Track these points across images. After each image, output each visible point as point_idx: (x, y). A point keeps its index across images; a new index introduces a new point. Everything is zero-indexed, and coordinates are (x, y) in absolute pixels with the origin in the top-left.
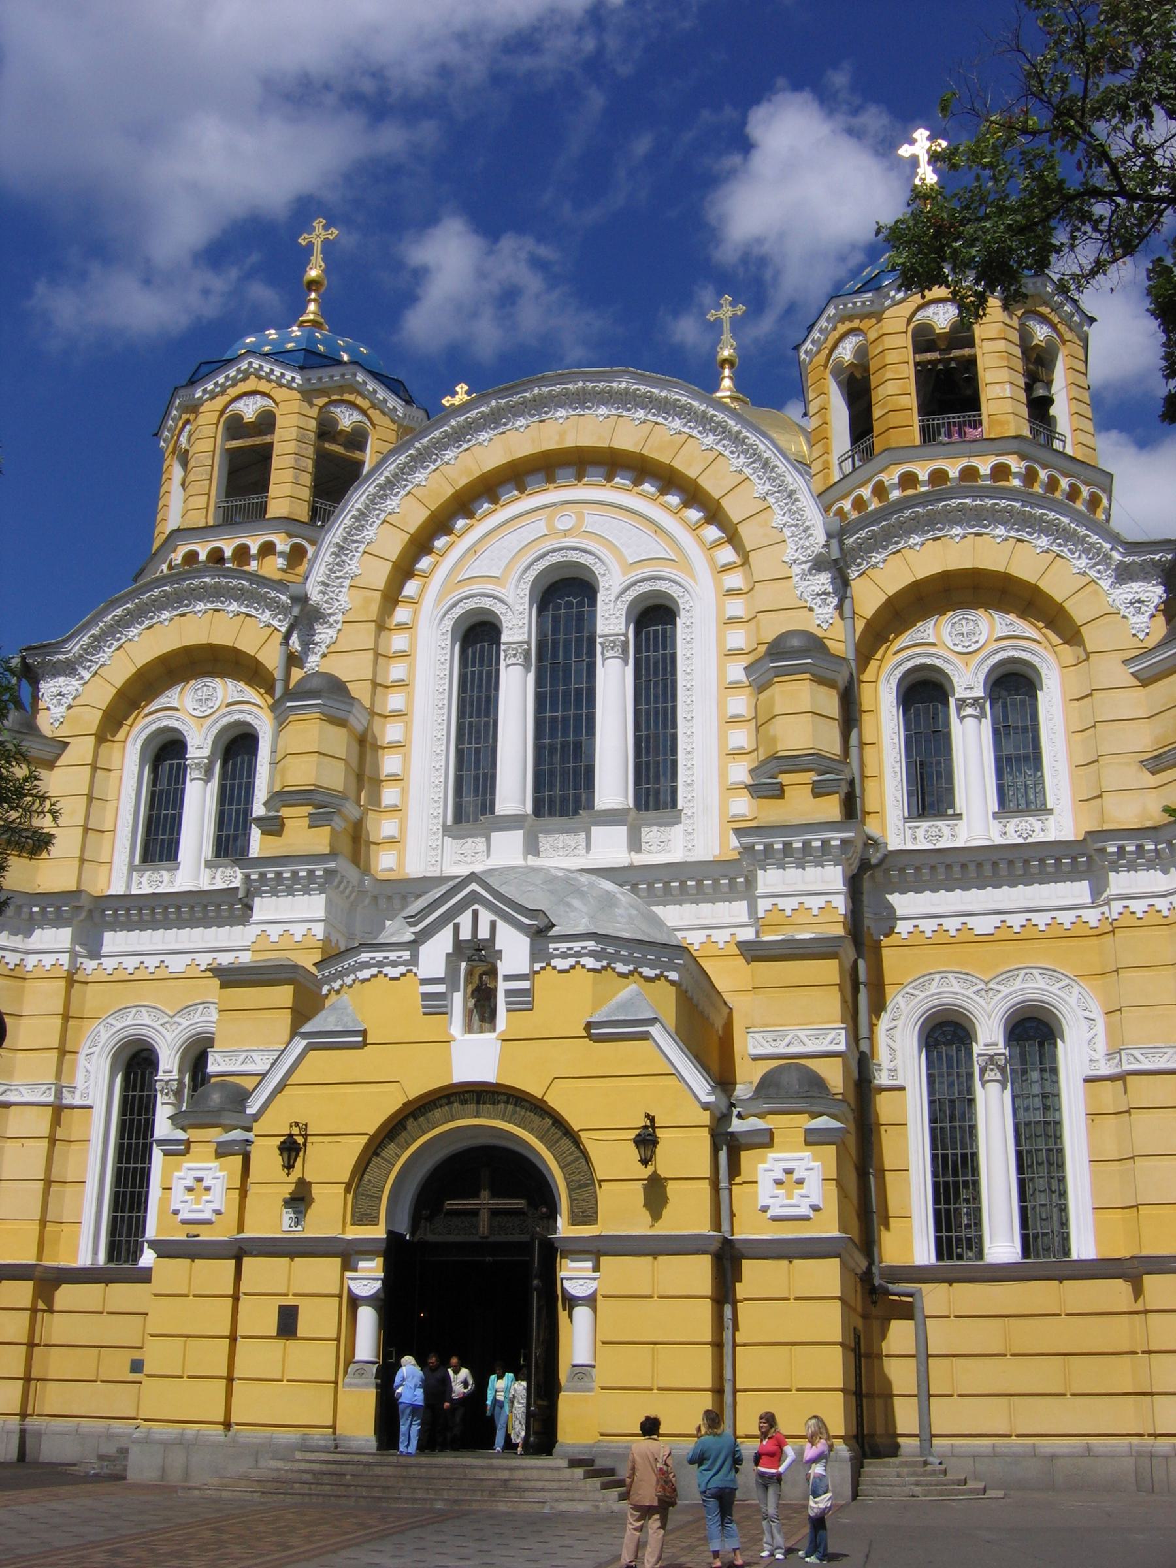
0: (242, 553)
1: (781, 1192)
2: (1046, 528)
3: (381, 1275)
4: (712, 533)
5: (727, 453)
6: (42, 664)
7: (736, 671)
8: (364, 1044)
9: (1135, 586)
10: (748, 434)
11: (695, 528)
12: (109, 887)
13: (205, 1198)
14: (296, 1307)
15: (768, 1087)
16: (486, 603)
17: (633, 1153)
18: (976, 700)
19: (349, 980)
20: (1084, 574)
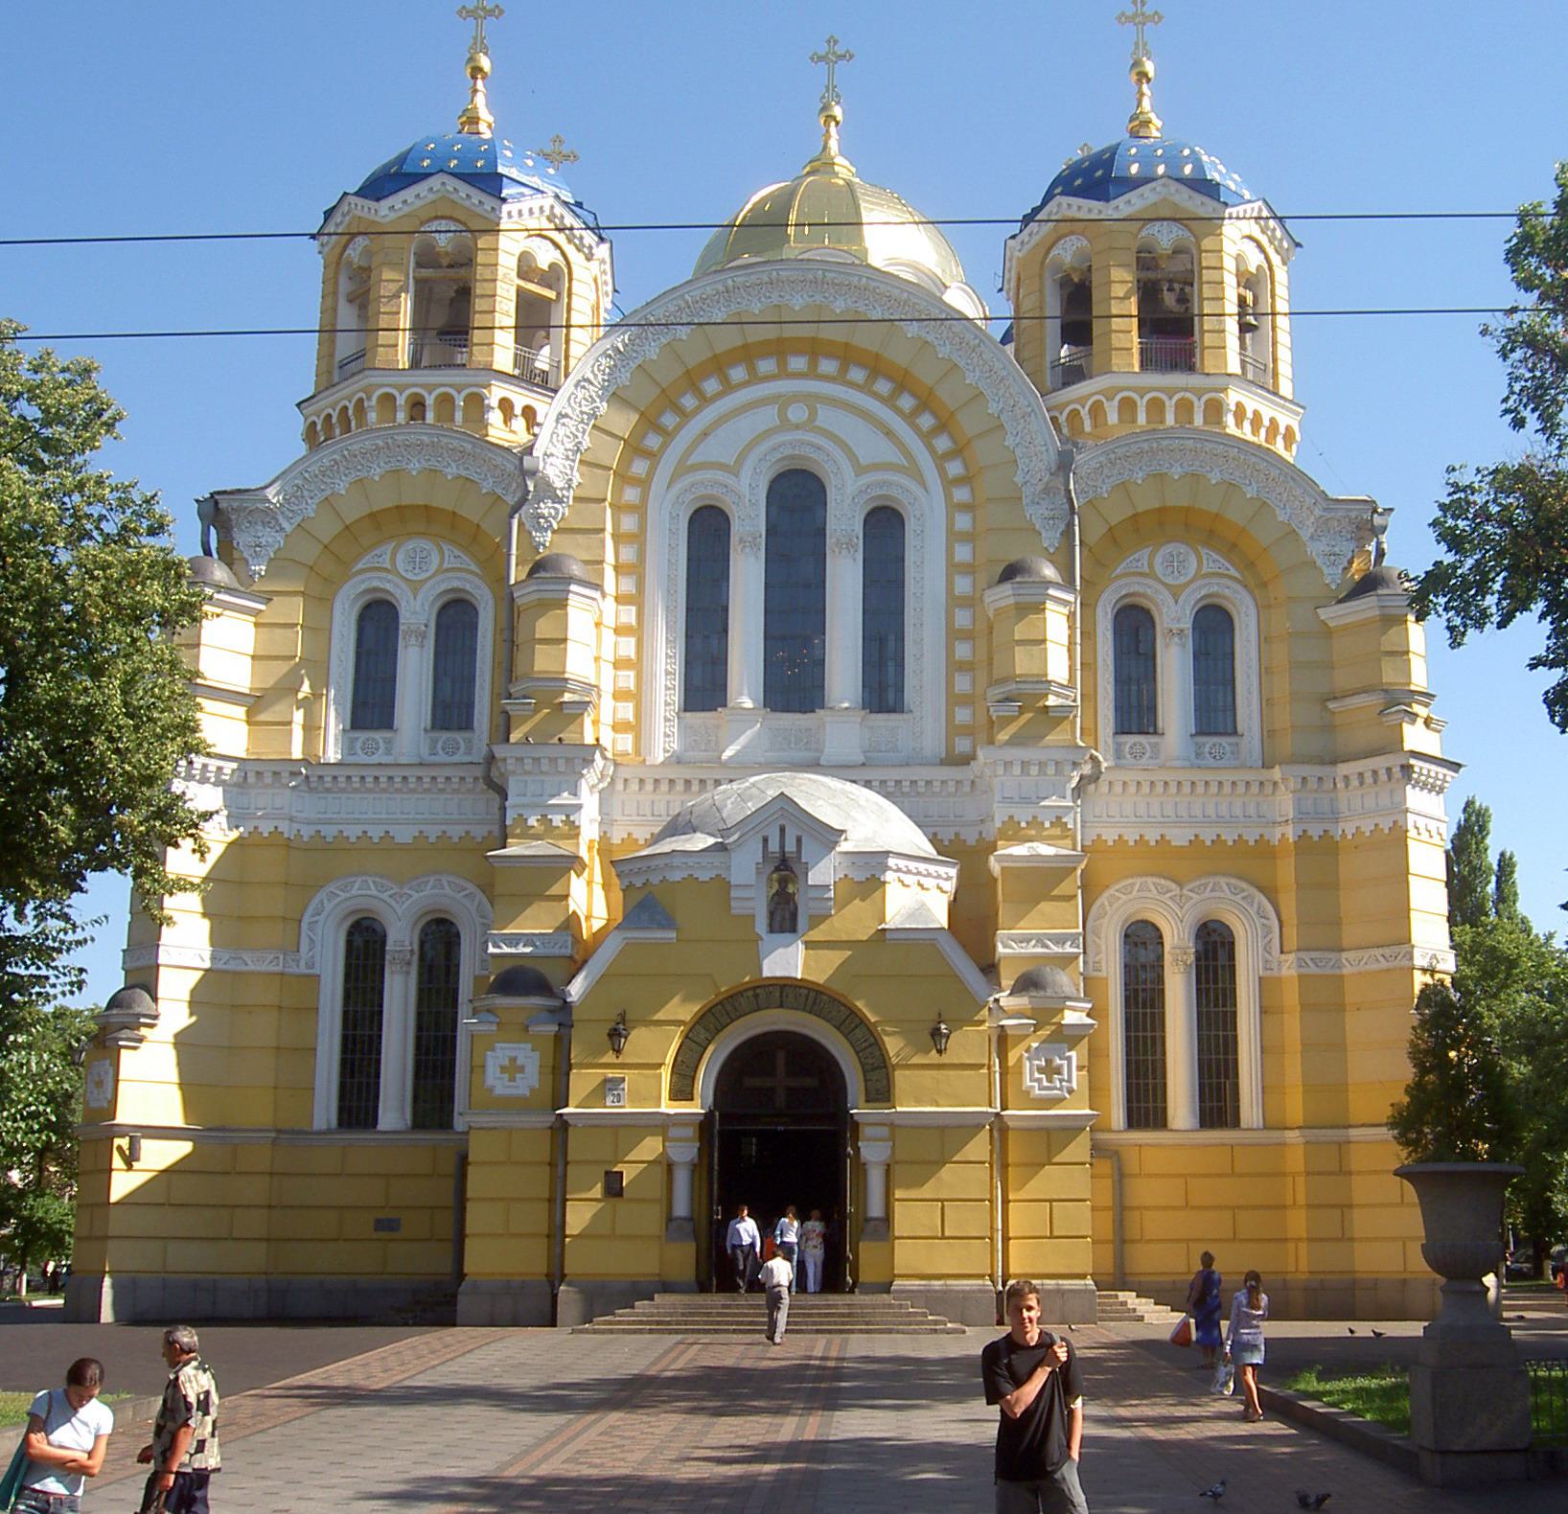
5: (962, 364)
13: (518, 1076)
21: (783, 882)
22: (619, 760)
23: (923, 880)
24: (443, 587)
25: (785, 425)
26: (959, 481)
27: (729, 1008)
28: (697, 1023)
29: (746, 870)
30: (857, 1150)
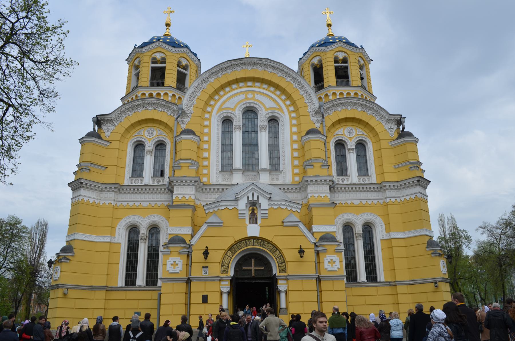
0: (158, 94)
1: (330, 265)
2: (370, 108)
3: (230, 286)
4: (288, 102)
5: (292, 83)
6: (103, 120)
7: (295, 138)
9: (390, 124)
10: (299, 79)
11: (283, 101)
12: (124, 183)
13: (176, 267)
14: (207, 295)
15: (322, 239)
16: (229, 115)
17: (299, 255)
18: (353, 149)
19: (216, 209)
20: (379, 121)
21: (253, 210)
22: (204, 184)
23: (293, 209)
24: (157, 140)
27: (238, 246)
28: (229, 250)
29: (242, 204)
30: (278, 287)
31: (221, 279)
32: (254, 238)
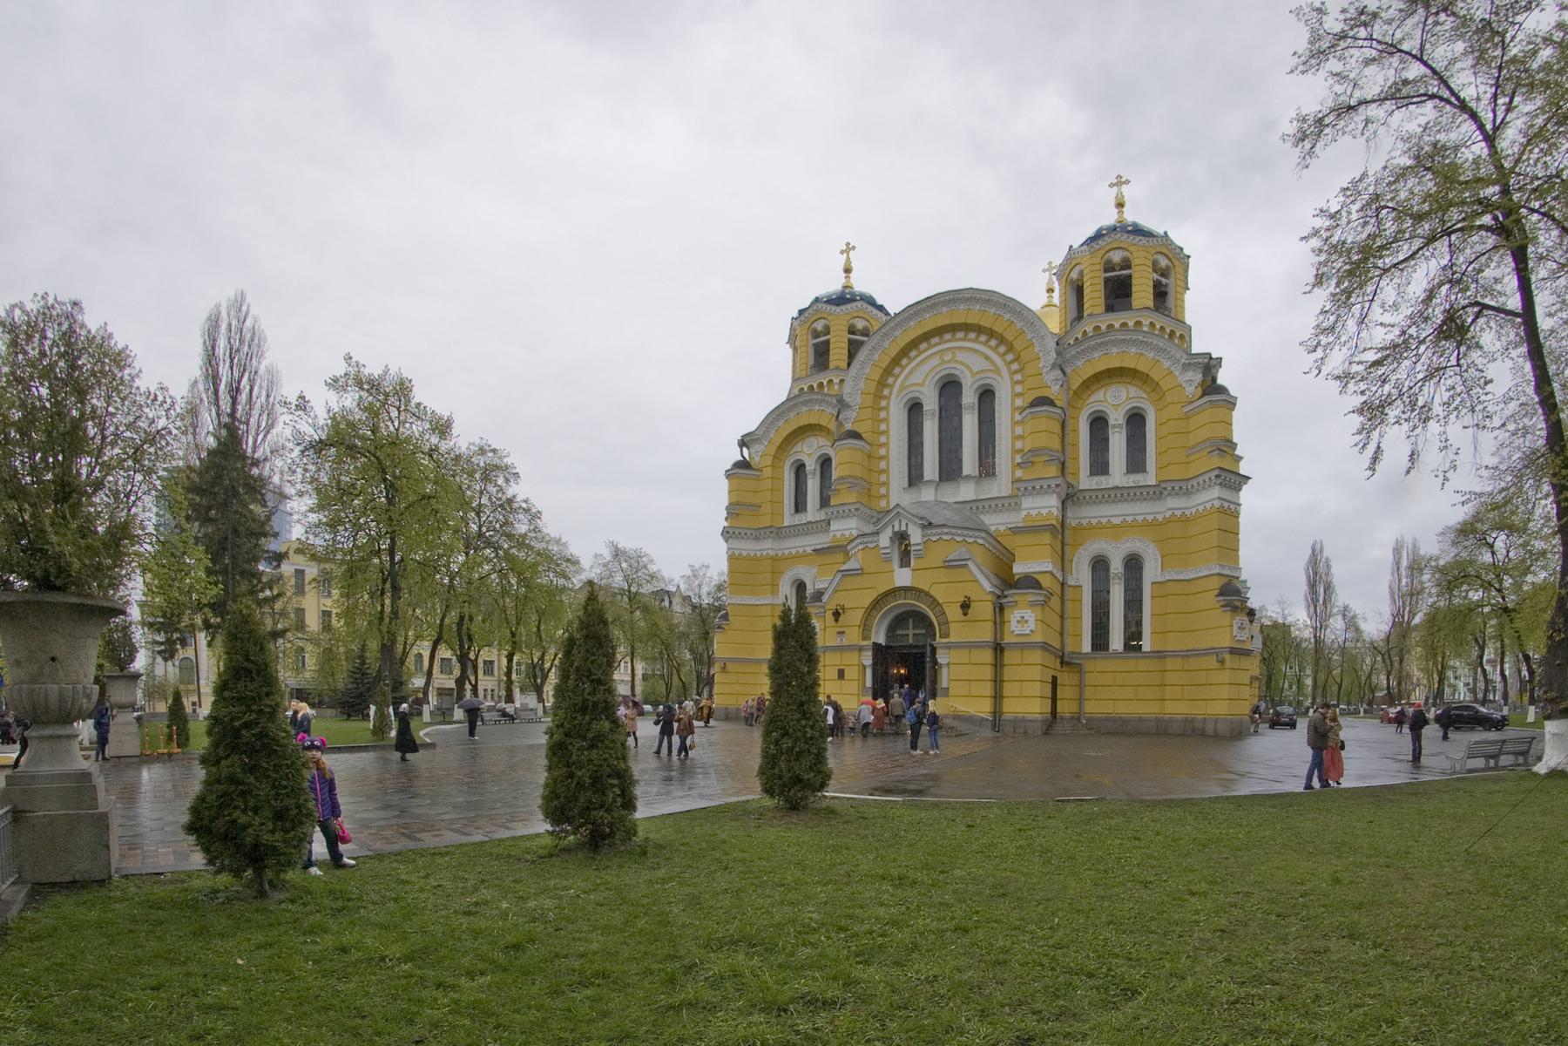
8: (862, 574)
16: (917, 395)
17: (960, 611)
25: (943, 362)
26: (1016, 372)
28: (874, 607)
29: (885, 540)
31: (861, 649)
32: (905, 590)
